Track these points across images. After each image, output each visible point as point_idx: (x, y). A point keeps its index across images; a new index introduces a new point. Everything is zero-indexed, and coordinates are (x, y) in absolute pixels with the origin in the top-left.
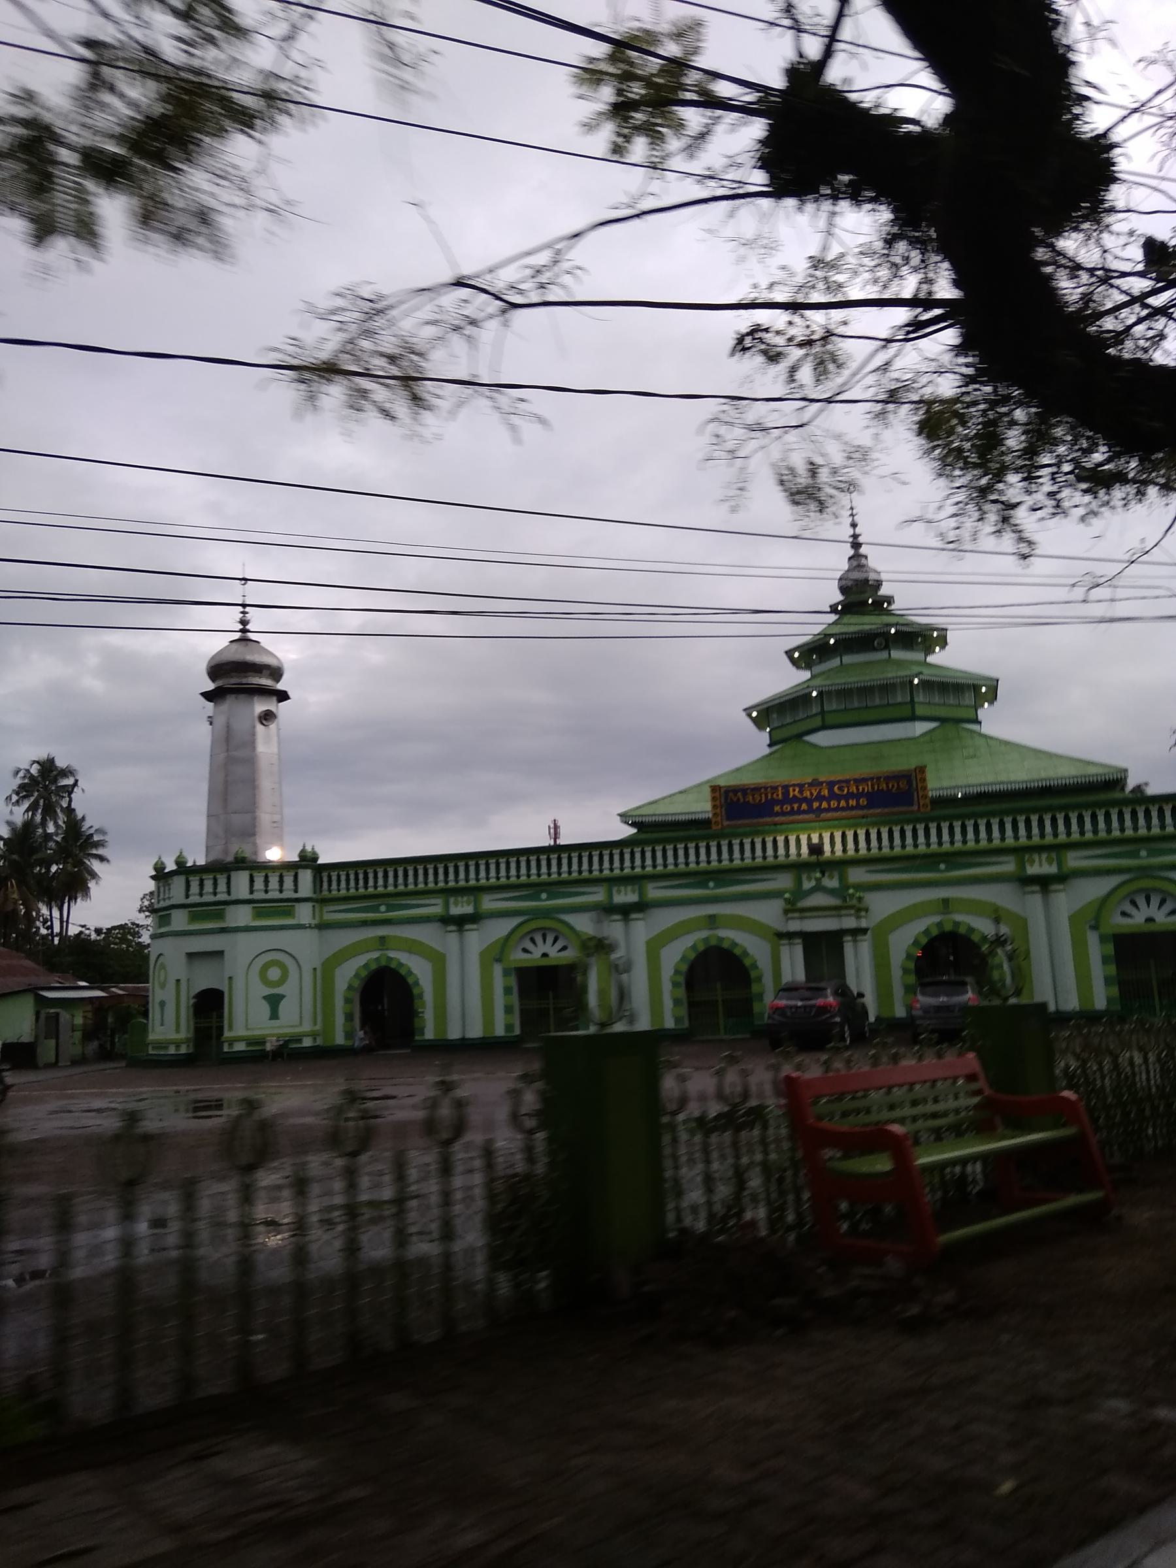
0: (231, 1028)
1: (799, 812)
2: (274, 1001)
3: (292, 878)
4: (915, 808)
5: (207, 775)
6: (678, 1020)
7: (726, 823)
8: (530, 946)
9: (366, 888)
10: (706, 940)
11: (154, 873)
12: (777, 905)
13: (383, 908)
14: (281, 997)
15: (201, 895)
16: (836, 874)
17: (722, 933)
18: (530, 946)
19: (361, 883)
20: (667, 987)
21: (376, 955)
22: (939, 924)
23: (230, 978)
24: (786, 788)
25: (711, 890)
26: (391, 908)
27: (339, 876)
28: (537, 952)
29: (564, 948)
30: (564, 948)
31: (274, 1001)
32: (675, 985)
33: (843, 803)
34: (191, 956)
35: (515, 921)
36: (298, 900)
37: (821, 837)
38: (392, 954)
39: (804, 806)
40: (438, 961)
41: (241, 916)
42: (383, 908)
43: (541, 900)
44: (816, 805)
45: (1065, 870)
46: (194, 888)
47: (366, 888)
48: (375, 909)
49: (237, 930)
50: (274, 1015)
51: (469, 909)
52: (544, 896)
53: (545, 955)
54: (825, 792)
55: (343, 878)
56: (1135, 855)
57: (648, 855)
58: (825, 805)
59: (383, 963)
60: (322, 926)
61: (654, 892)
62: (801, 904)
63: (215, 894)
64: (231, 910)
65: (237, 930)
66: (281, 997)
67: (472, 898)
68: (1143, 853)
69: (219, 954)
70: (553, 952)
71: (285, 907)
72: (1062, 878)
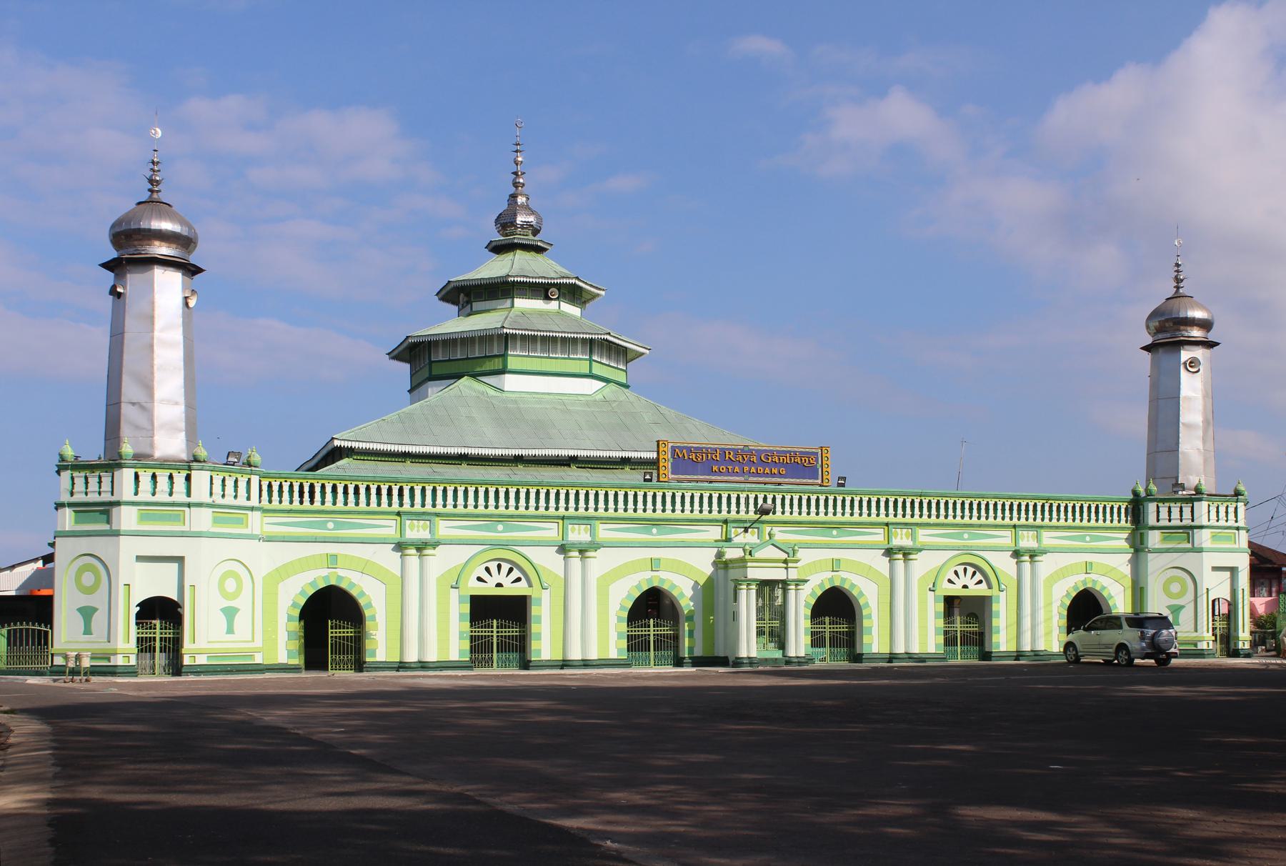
1: (734, 473)
2: (230, 613)
3: (245, 484)
4: (819, 481)
5: (125, 357)
6: (619, 650)
7: (671, 476)
8: (485, 576)
9: (312, 502)
10: (650, 580)
13: (331, 525)
14: (237, 610)
17: (662, 575)
18: (485, 576)
20: (613, 620)
21: (325, 572)
22: (831, 579)
24: (723, 451)
25: (655, 535)
26: (338, 526)
28: (492, 581)
31: (230, 613)
32: (619, 619)
33: (767, 470)
34: (140, 559)
36: (252, 509)
37: (765, 499)
38: (341, 573)
41: (201, 519)
45: (437, 537)
47: (312, 502)
48: (323, 526)
49: (198, 535)
50: (230, 630)
52: (500, 527)
53: (499, 585)
56: (960, 537)
58: (753, 470)
59: (333, 582)
60: (269, 539)
62: (757, 555)
65: (198, 535)
66: (237, 610)
68: (966, 536)
69: (180, 560)
70: (507, 582)
72: (595, 546)
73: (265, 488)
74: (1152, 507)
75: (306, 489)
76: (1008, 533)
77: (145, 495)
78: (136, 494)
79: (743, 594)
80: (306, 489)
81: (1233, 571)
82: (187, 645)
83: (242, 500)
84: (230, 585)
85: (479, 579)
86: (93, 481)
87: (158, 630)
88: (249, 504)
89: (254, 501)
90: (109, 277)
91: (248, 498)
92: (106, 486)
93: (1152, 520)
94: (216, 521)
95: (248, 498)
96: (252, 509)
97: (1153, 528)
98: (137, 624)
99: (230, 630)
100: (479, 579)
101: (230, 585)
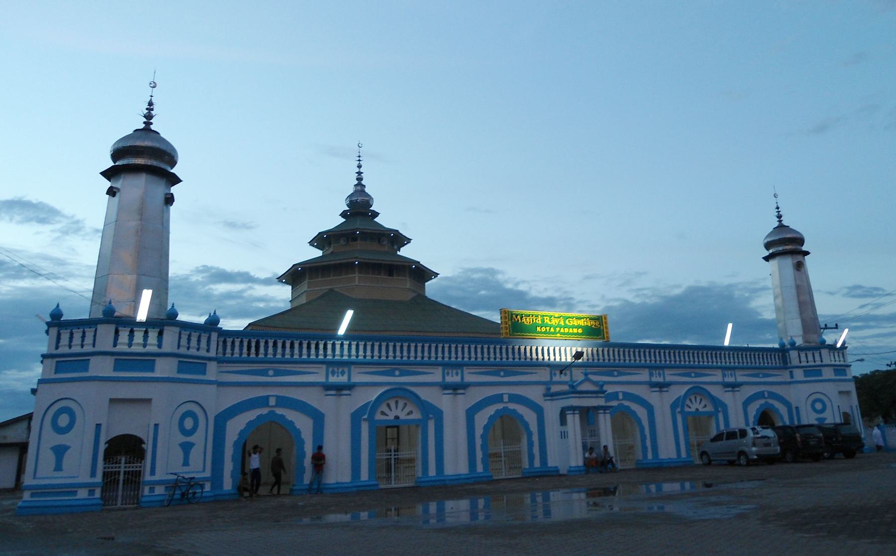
0: (153, 473)
8: (386, 410)
9: (257, 354)
11: (49, 320)
12: (541, 390)
13: (271, 373)
15: (130, 345)
16: (568, 373)
18: (386, 410)
19: (253, 350)
23: (156, 425)
26: (277, 373)
27: (233, 343)
29: (410, 413)
30: (410, 413)
34: (112, 401)
35: (381, 390)
36: (210, 359)
39: (552, 330)
40: (318, 419)
42: (271, 373)
43: (394, 376)
44: (558, 329)
46: (184, 341)
47: (257, 354)
48: (264, 373)
51: (343, 379)
53: (397, 417)
54: (562, 323)
55: (237, 344)
56: (689, 375)
57: (384, 348)
60: (221, 384)
61: (470, 377)
63: (145, 346)
64: (94, 361)
67: (346, 370)
69: (149, 401)
71: (146, 361)
73: (221, 344)
74: (794, 354)
75: (253, 344)
76: (719, 373)
77: (122, 347)
78: (115, 345)
79: (569, 418)
80: (253, 344)
81: (848, 393)
82: (148, 477)
83: (203, 353)
84: (189, 423)
85: (383, 413)
86: (77, 335)
87: (123, 466)
88: (208, 355)
89: (212, 354)
90: (107, 184)
91: (208, 351)
92: (89, 339)
93: (795, 362)
94: (180, 371)
95: (208, 351)
96: (210, 359)
97: (797, 367)
98: (105, 459)
99: (186, 463)
100: (383, 413)
101: (189, 423)
